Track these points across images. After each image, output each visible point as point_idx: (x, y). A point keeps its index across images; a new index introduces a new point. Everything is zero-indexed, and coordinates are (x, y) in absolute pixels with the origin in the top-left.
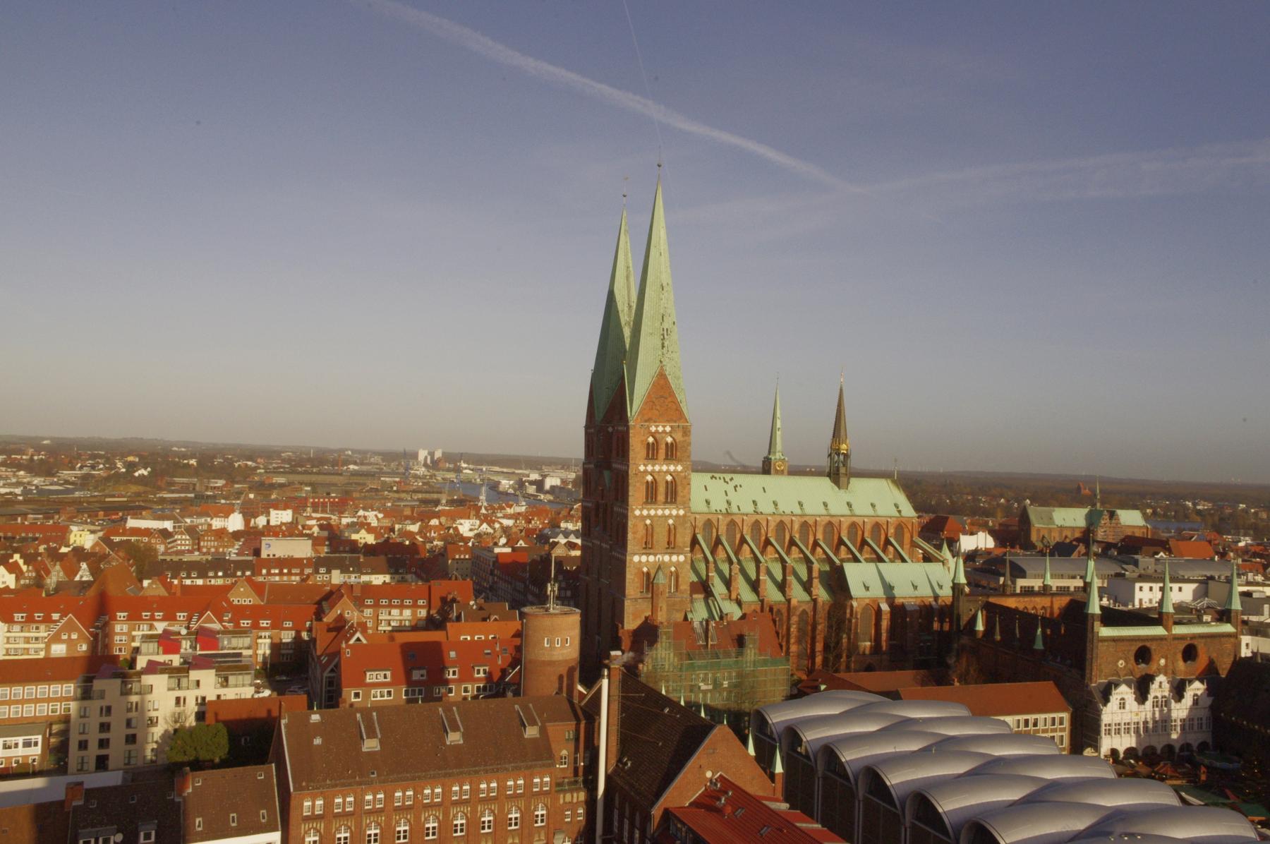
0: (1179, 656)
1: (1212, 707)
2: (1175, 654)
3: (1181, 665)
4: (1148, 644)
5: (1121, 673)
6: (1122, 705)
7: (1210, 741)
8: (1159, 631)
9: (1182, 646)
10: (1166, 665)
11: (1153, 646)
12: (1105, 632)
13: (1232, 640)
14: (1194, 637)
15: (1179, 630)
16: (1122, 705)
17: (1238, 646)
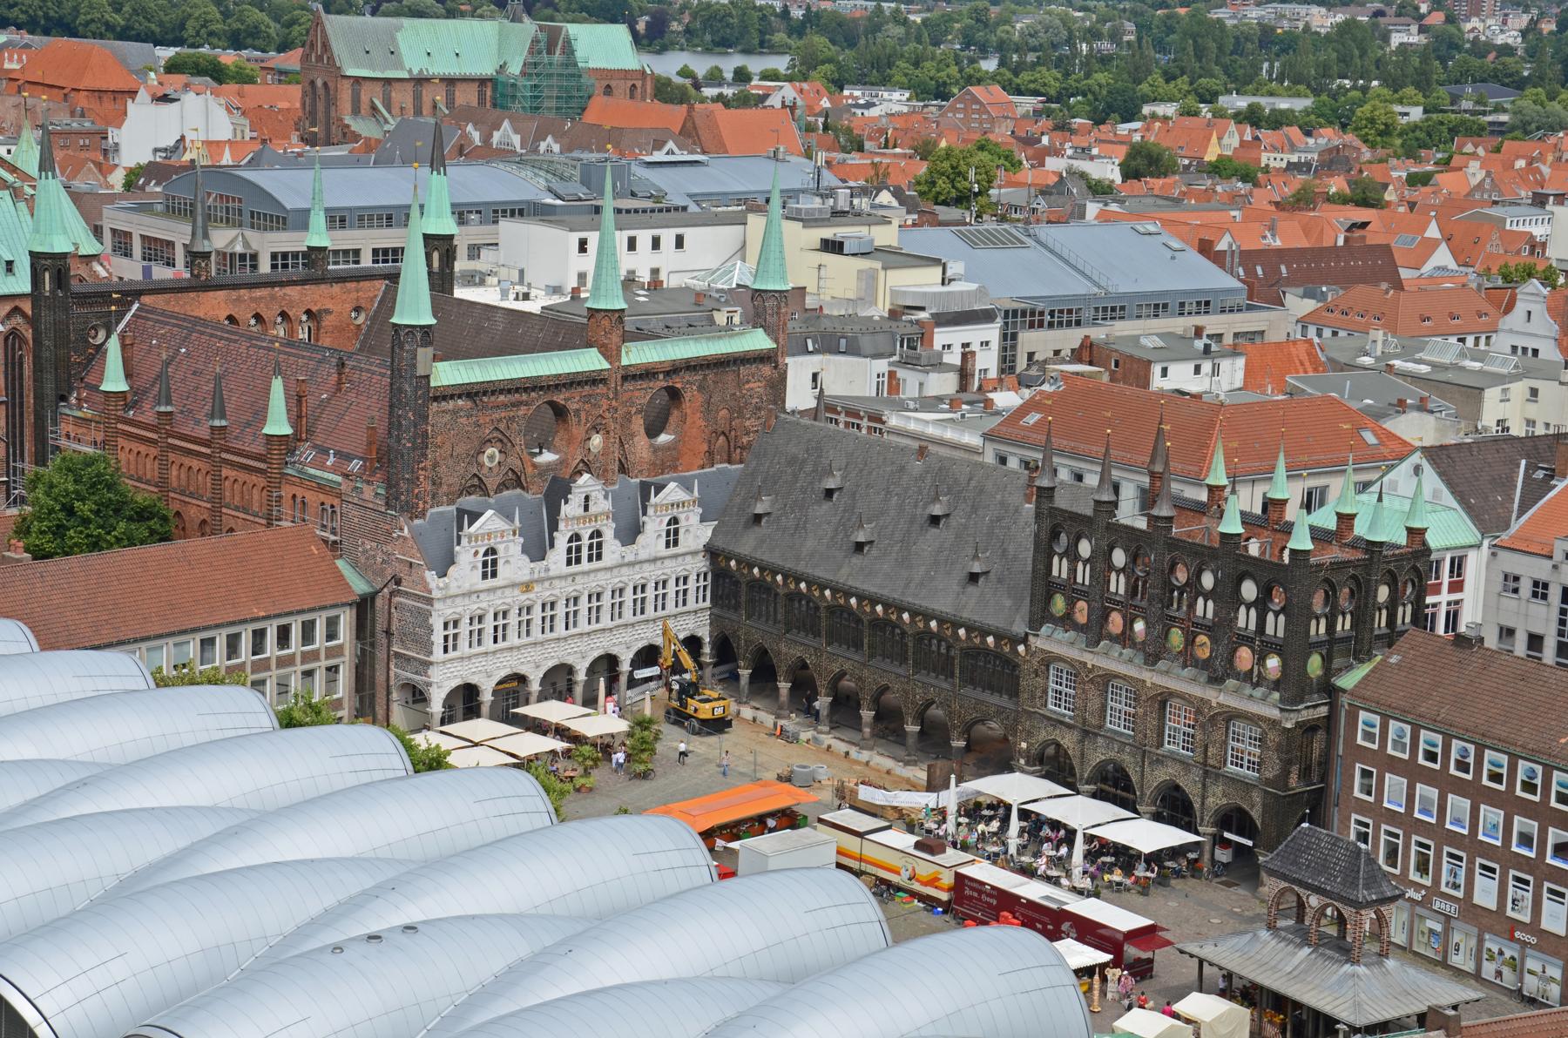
0: (638, 424)
1: (712, 552)
2: (628, 418)
3: (641, 446)
4: (559, 398)
5: (491, 483)
6: (490, 568)
7: (705, 633)
8: (589, 361)
9: (643, 394)
10: (605, 452)
11: (571, 400)
12: (447, 374)
13: (767, 370)
14: (676, 368)
15: (637, 355)
16: (490, 568)
17: (778, 386)
